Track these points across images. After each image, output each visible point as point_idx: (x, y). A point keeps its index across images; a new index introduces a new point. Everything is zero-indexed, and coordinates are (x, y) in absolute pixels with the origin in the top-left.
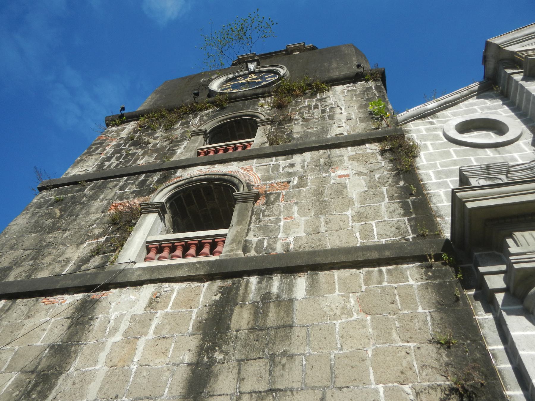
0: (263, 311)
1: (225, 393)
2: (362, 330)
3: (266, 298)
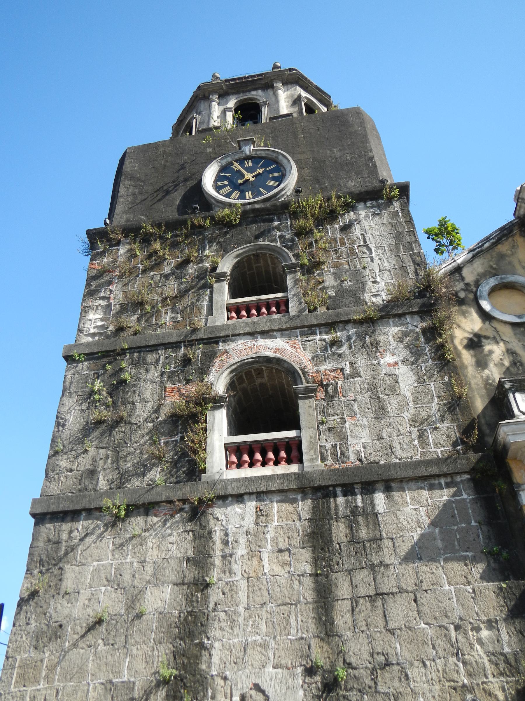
0: (355, 524)
1: (346, 598)
2: (433, 542)
3: (354, 511)
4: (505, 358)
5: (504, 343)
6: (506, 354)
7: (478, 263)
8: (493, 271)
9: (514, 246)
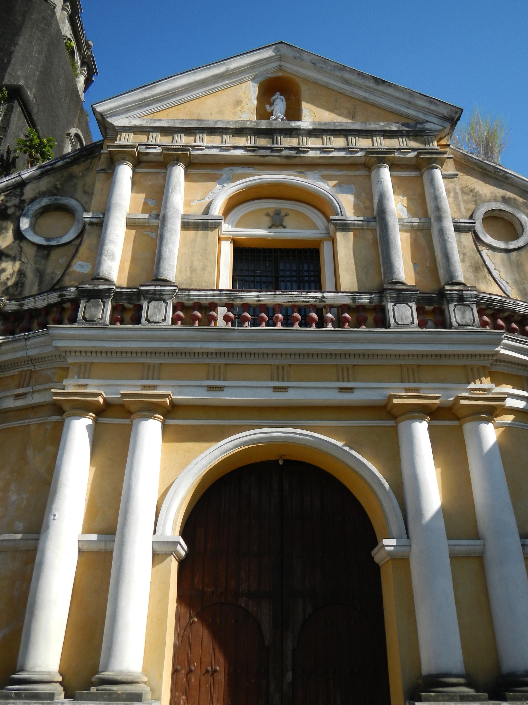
4: (12, 278)
5: (21, 264)
6: (15, 275)
7: (45, 181)
8: (55, 191)
9: (88, 168)
